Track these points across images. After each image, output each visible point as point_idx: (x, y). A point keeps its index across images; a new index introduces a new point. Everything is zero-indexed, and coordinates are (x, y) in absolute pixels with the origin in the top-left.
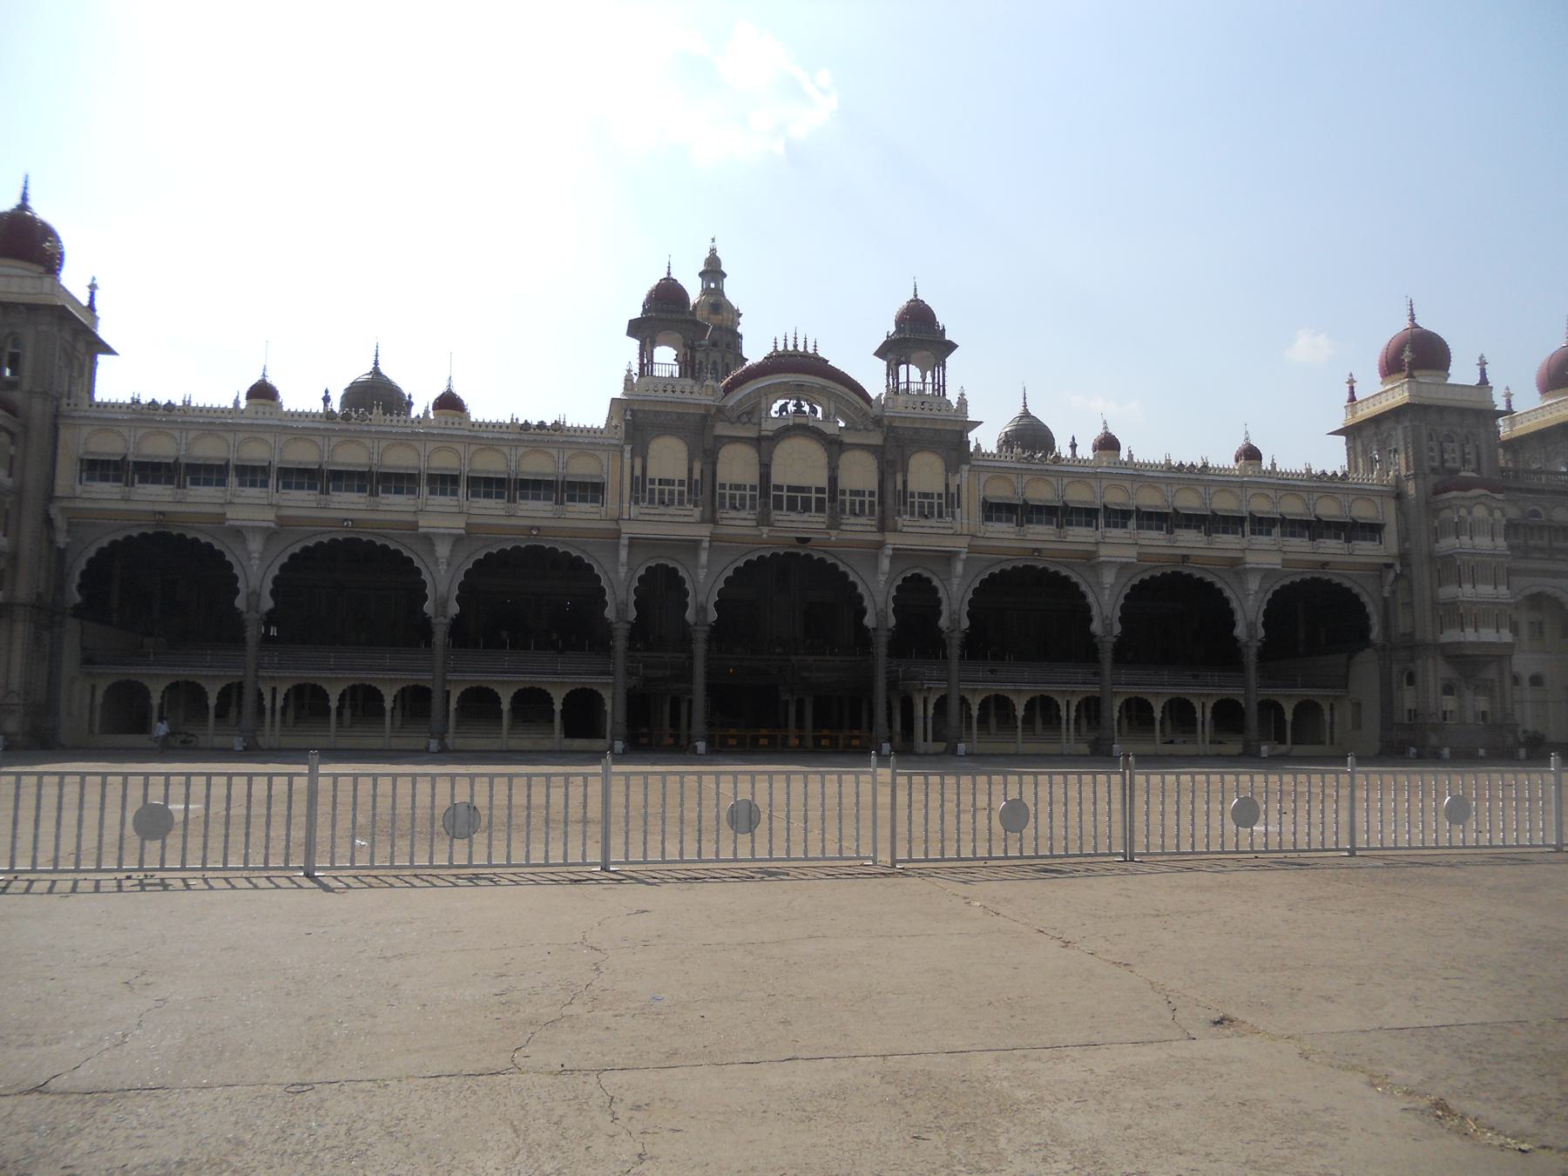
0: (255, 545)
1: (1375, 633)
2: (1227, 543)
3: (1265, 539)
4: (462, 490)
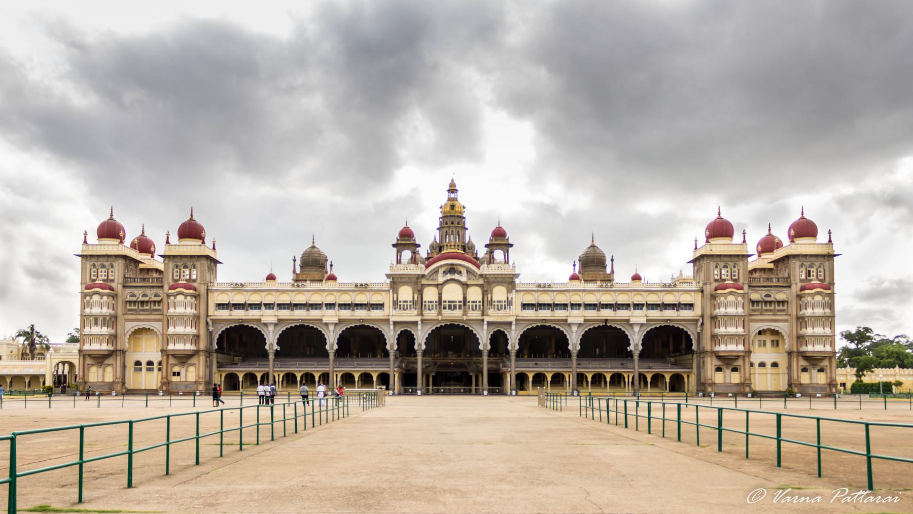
0: (271, 328)
1: (694, 347)
2: (622, 314)
3: (640, 311)
4: (337, 308)
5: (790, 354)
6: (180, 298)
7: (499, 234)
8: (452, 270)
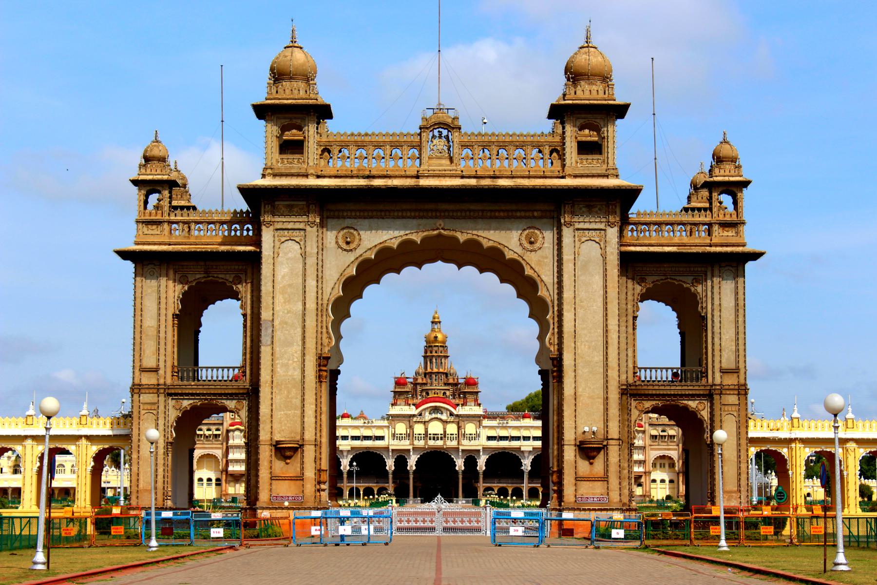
5: (678, 474)
6: (237, 433)
7: (471, 382)
8: (436, 410)
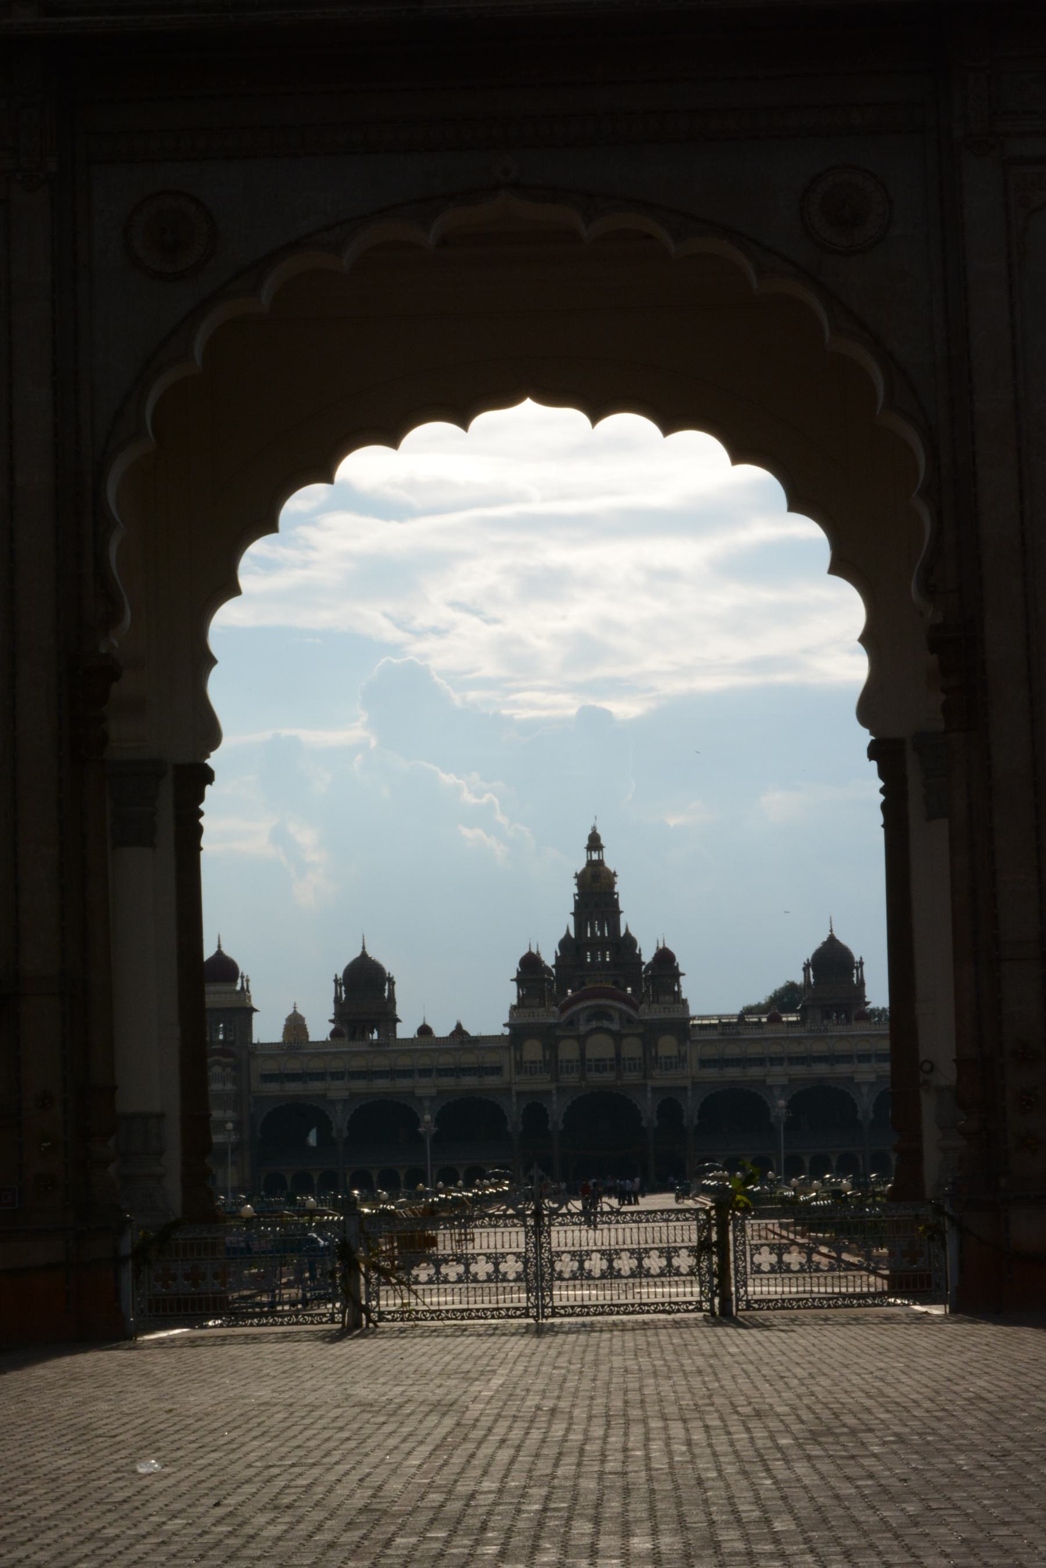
2: (843, 1069)
7: (665, 958)
8: (600, 1014)
